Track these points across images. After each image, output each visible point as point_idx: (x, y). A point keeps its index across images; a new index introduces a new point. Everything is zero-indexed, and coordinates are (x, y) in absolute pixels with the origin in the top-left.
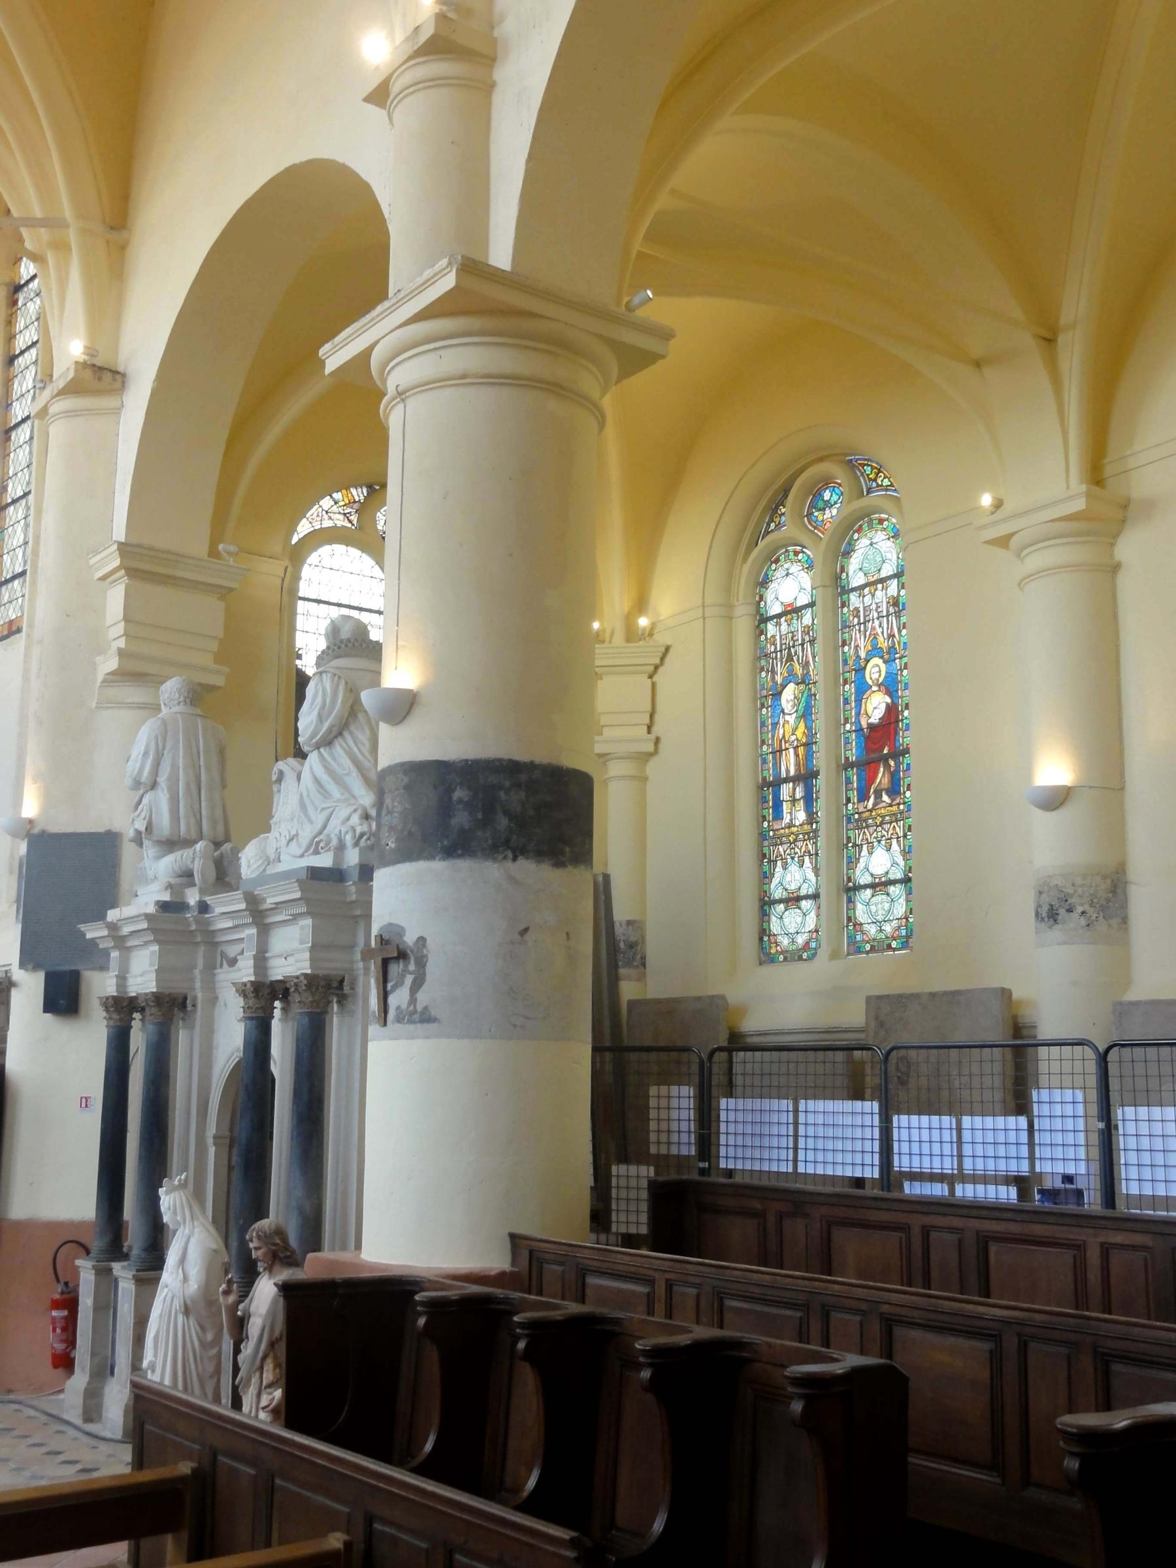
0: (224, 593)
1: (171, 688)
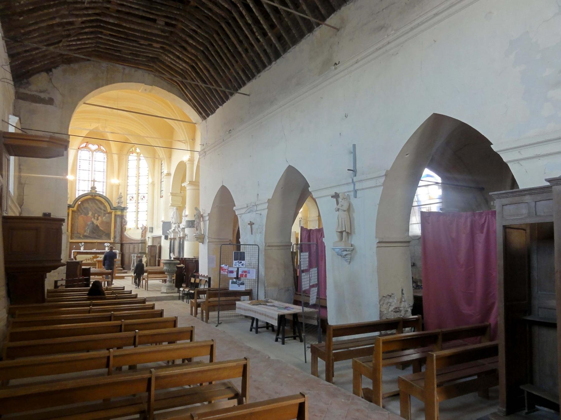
0: (182, 197)
1: (175, 208)
